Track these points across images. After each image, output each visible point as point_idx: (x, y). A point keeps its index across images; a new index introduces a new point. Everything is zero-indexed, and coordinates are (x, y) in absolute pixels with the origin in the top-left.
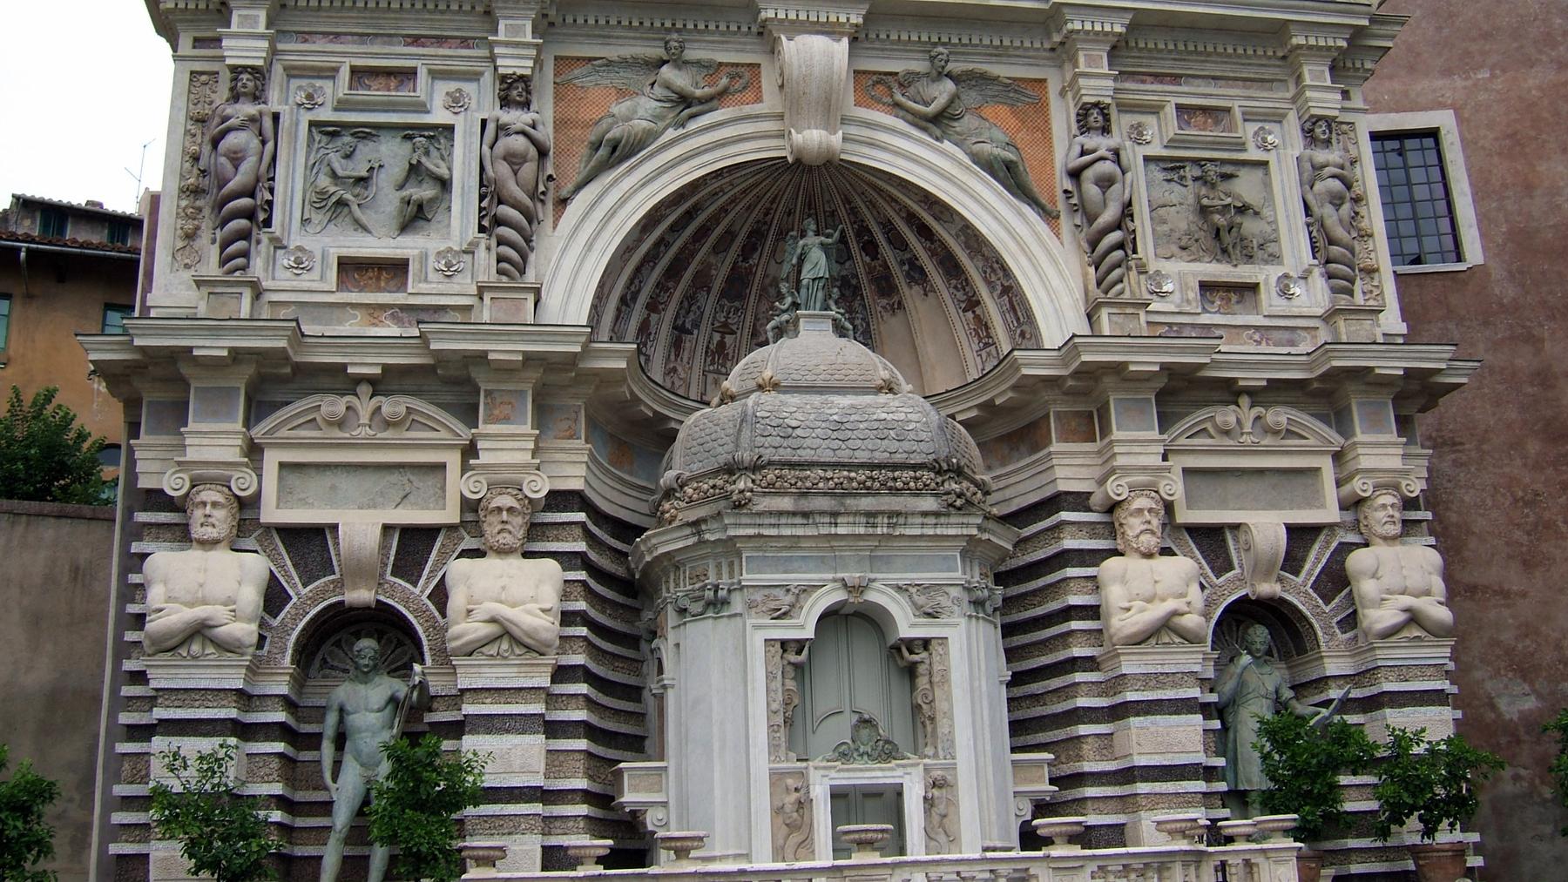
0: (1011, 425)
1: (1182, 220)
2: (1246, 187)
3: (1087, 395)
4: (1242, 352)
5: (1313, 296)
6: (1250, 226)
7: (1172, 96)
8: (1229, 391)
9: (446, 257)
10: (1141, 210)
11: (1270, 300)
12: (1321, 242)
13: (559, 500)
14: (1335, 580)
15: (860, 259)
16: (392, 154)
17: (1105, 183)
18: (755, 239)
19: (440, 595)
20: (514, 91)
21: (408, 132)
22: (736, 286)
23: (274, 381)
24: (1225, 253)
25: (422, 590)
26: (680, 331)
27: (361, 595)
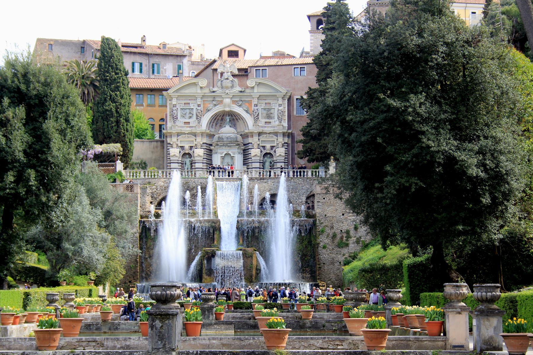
0: (245, 136)
1: (265, 115)
2: (272, 111)
3: (252, 134)
4: (268, 129)
5: (277, 123)
6: (272, 115)
7: (265, 102)
8: (266, 133)
9: (193, 121)
10: (260, 115)
11: (273, 124)
12: (278, 117)
13: (203, 143)
14: (275, 152)
15: (234, 117)
16: (188, 111)
17: (256, 112)
18: (223, 115)
19: (193, 152)
20: (199, 106)
21: (189, 109)
22: (222, 119)
23: (178, 135)
24: (268, 119)
25: (192, 151)
26: (216, 124)
27: (187, 152)
